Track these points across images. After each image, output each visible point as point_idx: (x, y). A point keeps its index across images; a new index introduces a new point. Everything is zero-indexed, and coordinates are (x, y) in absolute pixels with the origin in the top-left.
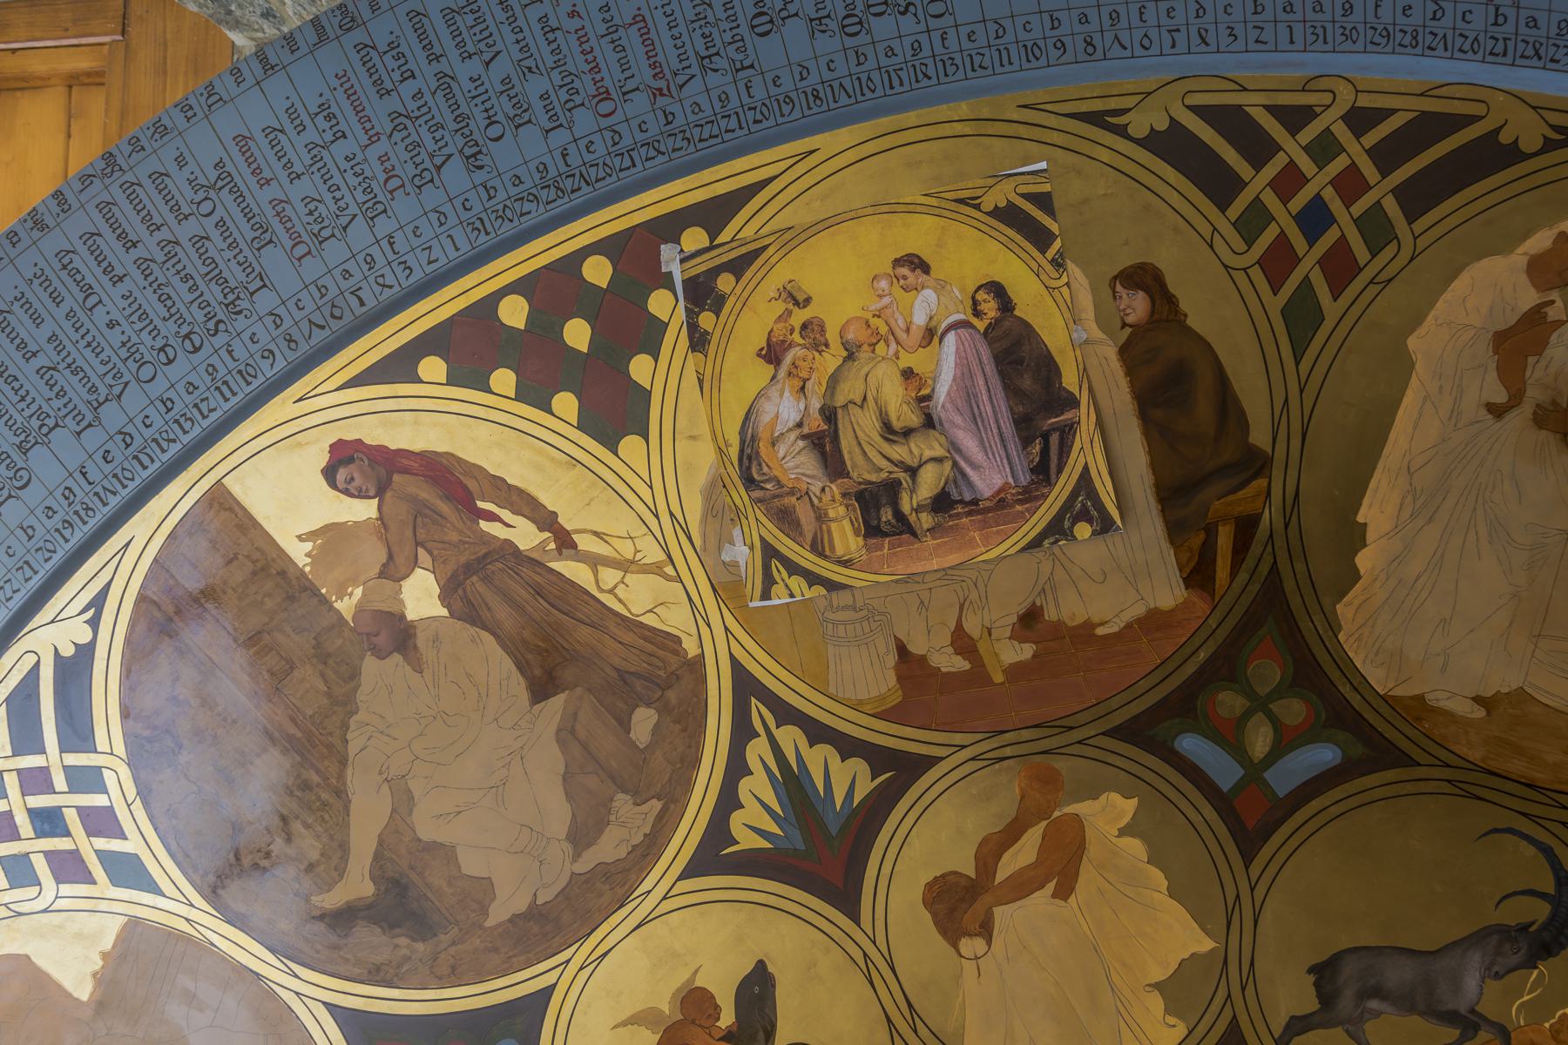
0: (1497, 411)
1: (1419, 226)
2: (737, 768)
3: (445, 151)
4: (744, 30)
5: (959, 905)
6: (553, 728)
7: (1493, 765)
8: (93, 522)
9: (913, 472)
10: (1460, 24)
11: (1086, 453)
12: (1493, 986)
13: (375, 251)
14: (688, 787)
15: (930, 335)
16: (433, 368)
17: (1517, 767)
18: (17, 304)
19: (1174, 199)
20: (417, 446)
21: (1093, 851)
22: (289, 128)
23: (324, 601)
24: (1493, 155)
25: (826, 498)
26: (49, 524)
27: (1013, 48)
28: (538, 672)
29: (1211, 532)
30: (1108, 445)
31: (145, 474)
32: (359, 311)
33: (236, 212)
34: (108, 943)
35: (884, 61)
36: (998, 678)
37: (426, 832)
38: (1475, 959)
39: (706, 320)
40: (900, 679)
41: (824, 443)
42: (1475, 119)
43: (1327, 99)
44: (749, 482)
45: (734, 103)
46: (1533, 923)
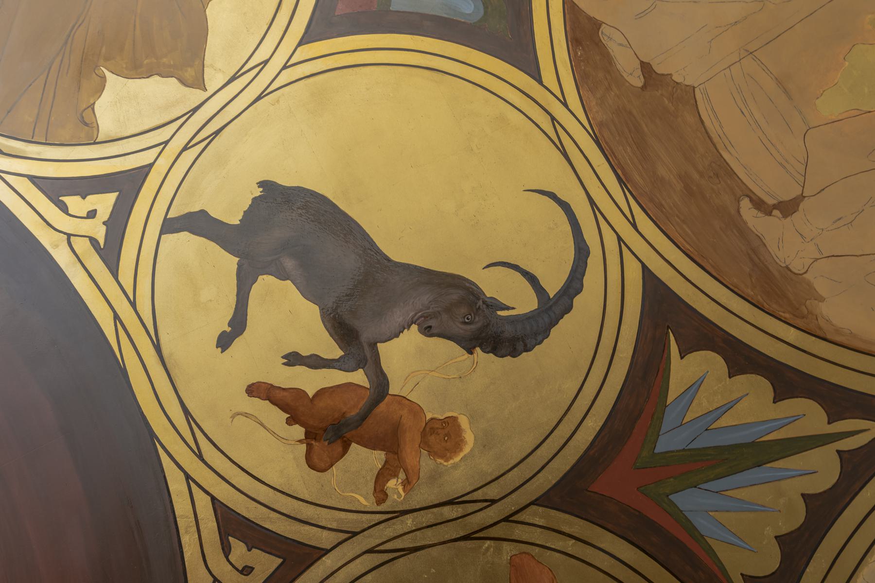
12: (412, 336)
38: (424, 299)
46: (508, 308)
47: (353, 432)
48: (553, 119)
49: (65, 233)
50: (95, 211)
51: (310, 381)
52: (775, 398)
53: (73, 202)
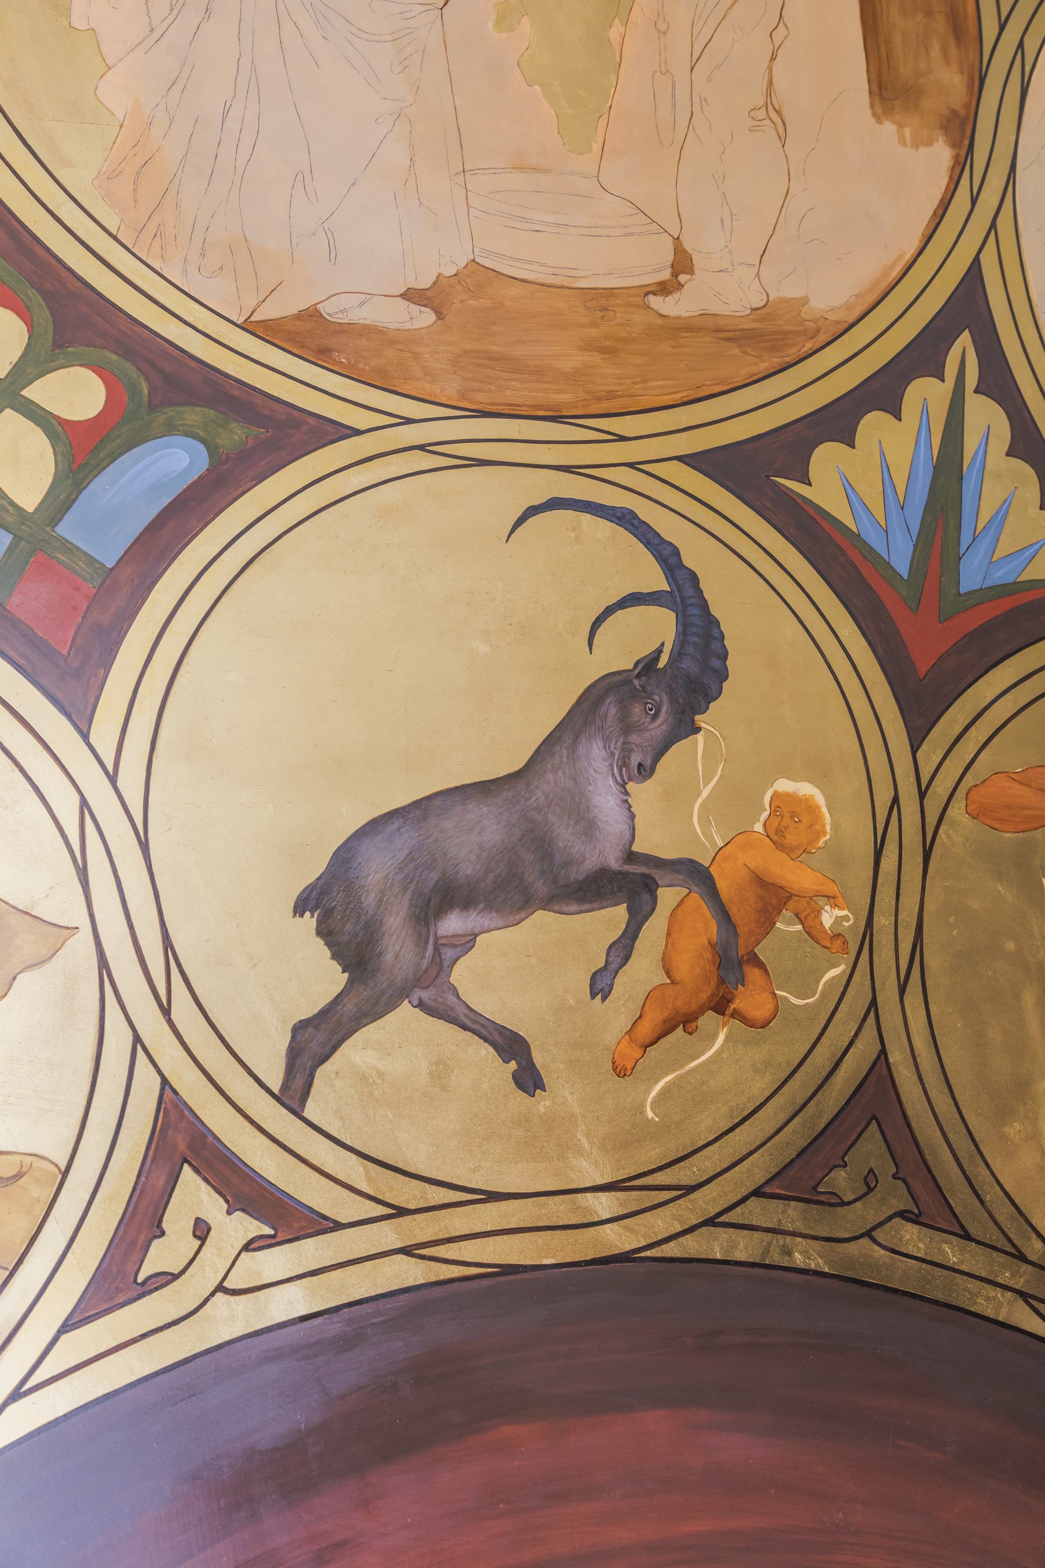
12: (641, 793)
17: (519, 392)
38: (596, 756)
46: (659, 651)
47: (741, 942)
48: (422, 448)
49: (213, 1294)
50: (198, 1220)
52: (896, 417)
53: (159, 1258)
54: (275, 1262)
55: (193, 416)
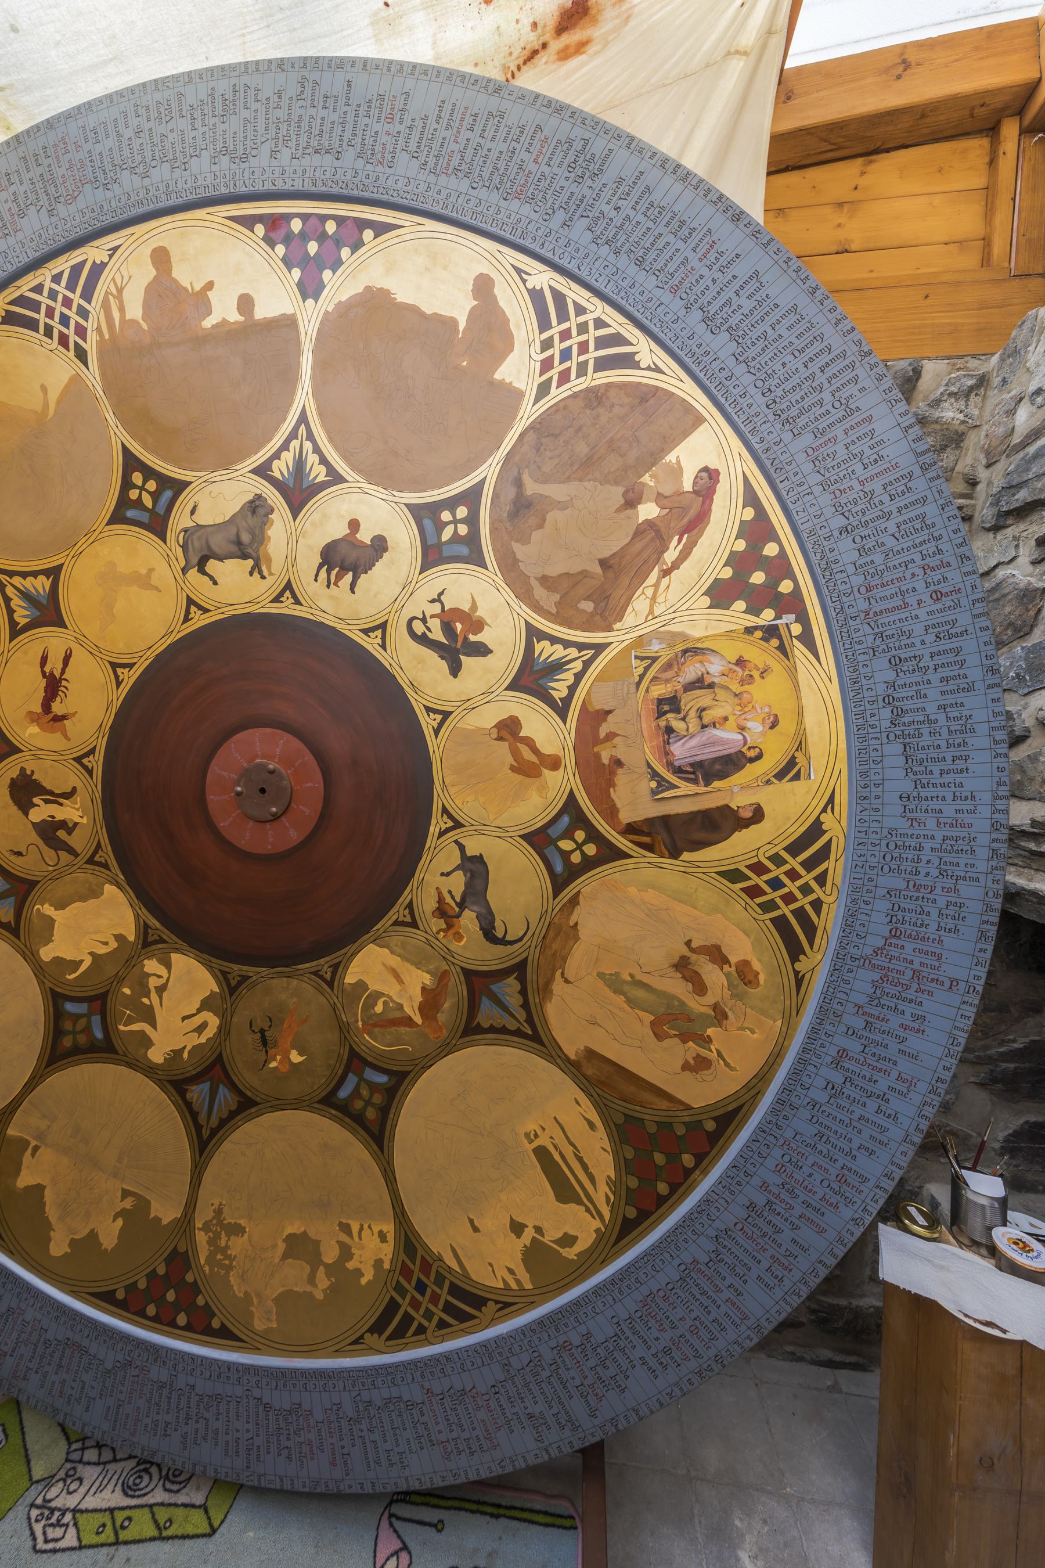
0: (688, 943)
1: (768, 923)
2: (567, 644)
3: (851, 517)
4: (893, 652)
5: (509, 728)
6: (588, 569)
7: (552, 926)
8: (693, 367)
9: (684, 719)
10: (853, 944)
11: (685, 788)
13: (806, 486)
14: (561, 624)
15: (742, 729)
16: (749, 514)
17: (551, 934)
18: (798, 316)
19: (792, 830)
20: (714, 507)
21: (527, 780)
22: (873, 442)
23: (650, 469)
24: (795, 951)
25: (675, 683)
26: (694, 346)
27: (867, 767)
28: (612, 562)
29: (648, 834)
30: (688, 798)
31: (712, 388)
32: (778, 481)
33: (833, 419)
34: (515, 384)
35: (868, 713)
36: (596, 749)
37: (550, 516)
38: (483, 911)
39: (759, 634)
40: (598, 711)
41: (699, 683)
42: (811, 947)
43: (828, 892)
44: (685, 652)
45: (857, 647)
51: (448, 899)
54: (437, 830)
55: (566, 875)
